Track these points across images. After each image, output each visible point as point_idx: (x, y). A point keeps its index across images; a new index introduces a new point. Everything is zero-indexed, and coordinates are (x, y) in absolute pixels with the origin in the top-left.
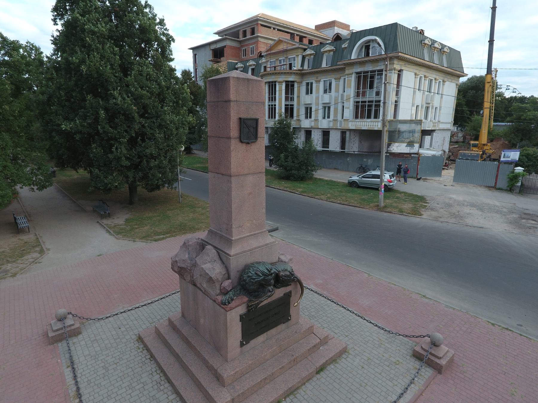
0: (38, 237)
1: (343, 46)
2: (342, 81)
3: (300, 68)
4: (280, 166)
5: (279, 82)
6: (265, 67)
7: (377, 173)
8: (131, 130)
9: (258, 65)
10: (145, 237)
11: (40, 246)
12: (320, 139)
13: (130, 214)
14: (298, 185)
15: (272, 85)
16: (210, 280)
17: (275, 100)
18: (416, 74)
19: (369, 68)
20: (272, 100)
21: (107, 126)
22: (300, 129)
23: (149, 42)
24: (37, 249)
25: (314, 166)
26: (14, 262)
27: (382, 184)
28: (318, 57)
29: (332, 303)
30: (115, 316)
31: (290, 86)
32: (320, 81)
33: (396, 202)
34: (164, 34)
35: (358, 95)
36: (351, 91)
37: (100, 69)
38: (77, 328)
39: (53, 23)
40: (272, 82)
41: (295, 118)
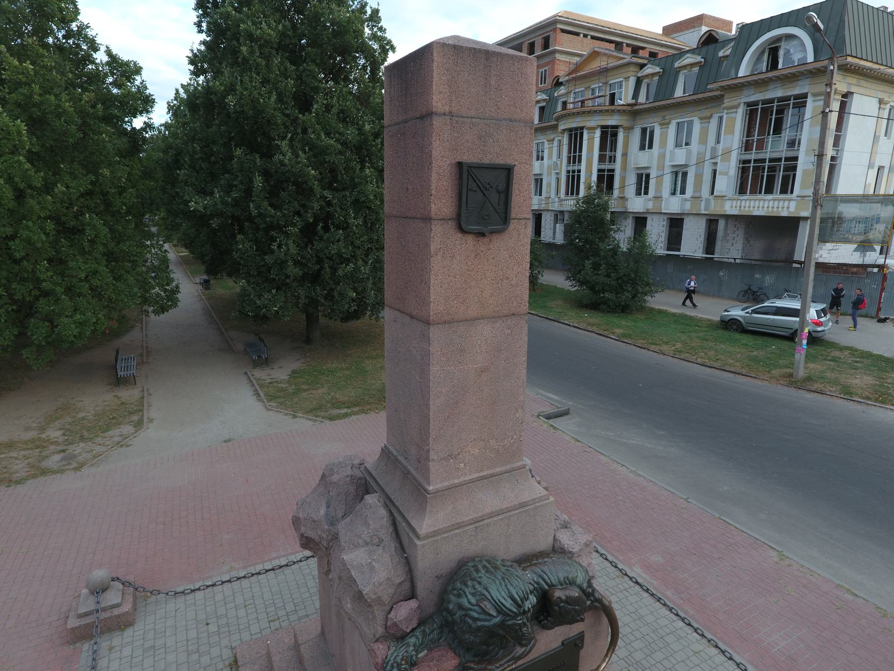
0: (145, 395)
1: (721, 54)
2: (714, 122)
3: (630, 100)
4: (582, 283)
5: (589, 129)
6: (565, 104)
7: (796, 305)
8: (306, 212)
9: (552, 101)
10: (315, 409)
11: (140, 413)
12: (663, 234)
13: (303, 361)
14: (616, 320)
15: (576, 135)
16: (359, 597)
17: (580, 161)
18: (881, 102)
19: (776, 92)
20: (574, 162)
21: (265, 203)
22: (624, 214)
23: (346, 52)
24: (135, 418)
25: (648, 284)
26: (91, 439)
27: (802, 331)
28: (668, 77)
29: (688, 630)
30: (210, 589)
31: (609, 136)
32: (669, 123)
33: (833, 370)
34: (374, 37)
35: (747, 147)
36: (734, 139)
37: (259, 103)
38: (123, 614)
39: (196, 29)
40: (576, 129)
41: (616, 193)
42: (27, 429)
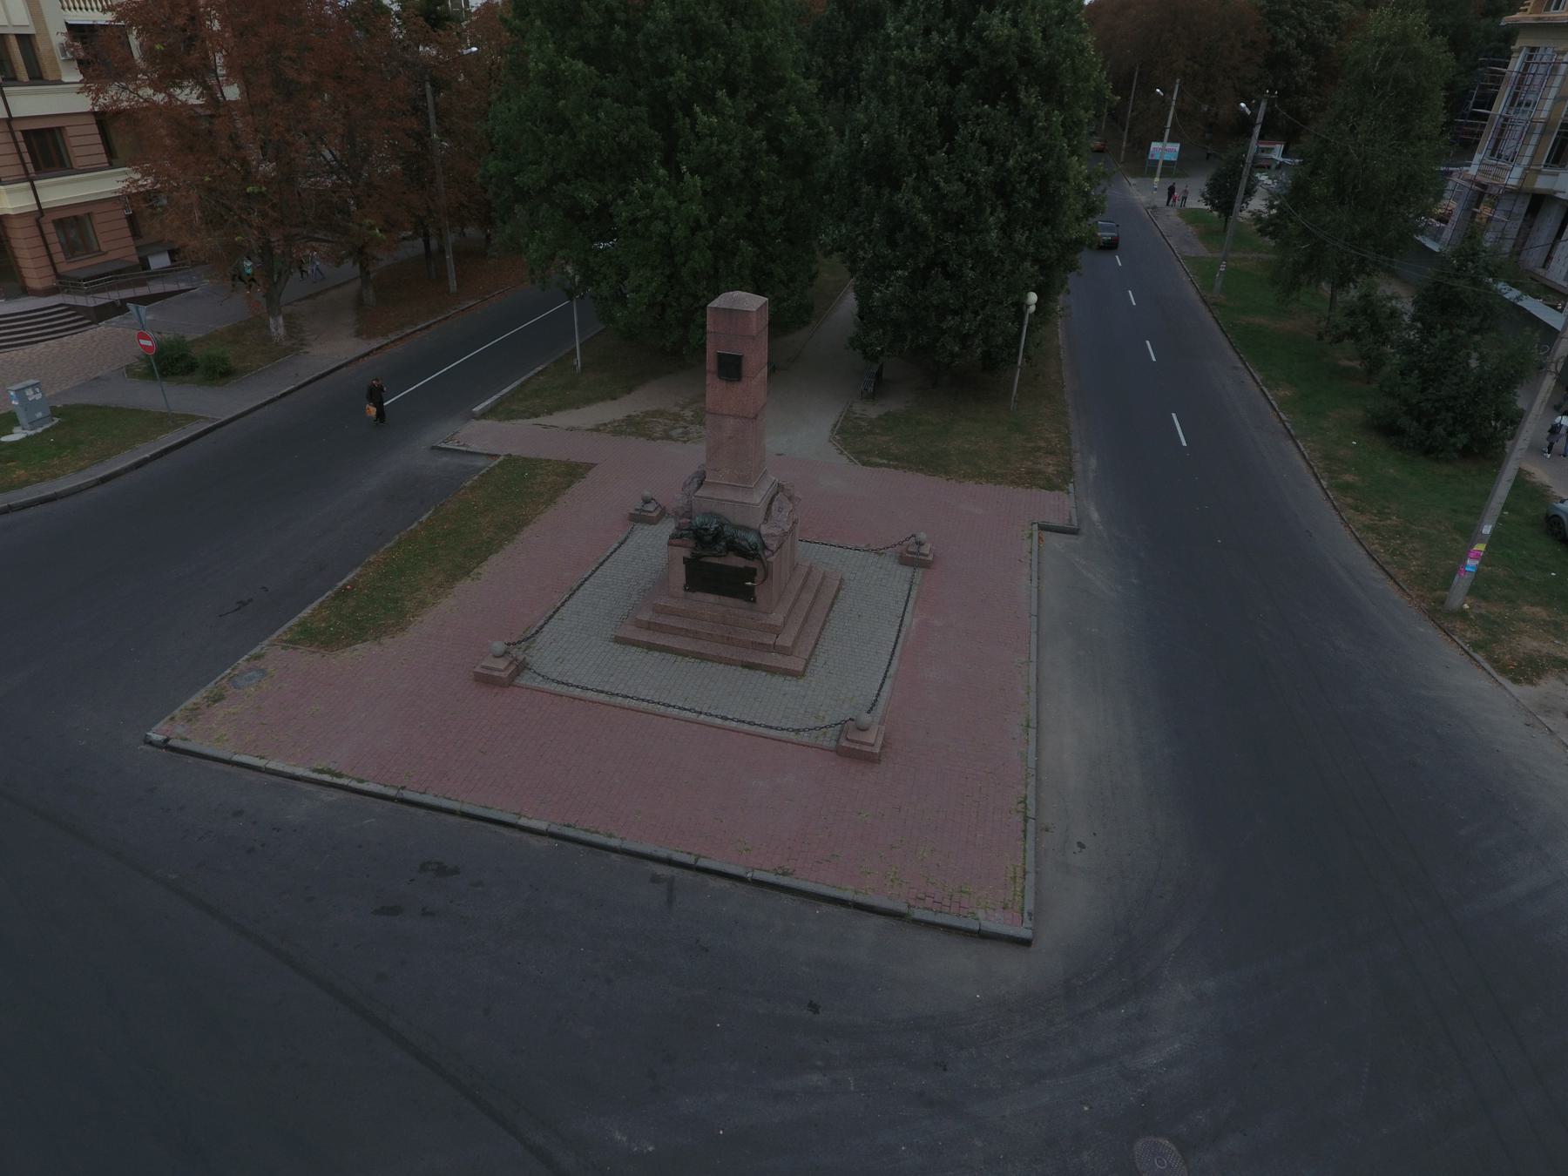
42: (676, 405)
